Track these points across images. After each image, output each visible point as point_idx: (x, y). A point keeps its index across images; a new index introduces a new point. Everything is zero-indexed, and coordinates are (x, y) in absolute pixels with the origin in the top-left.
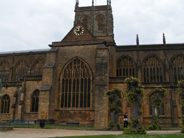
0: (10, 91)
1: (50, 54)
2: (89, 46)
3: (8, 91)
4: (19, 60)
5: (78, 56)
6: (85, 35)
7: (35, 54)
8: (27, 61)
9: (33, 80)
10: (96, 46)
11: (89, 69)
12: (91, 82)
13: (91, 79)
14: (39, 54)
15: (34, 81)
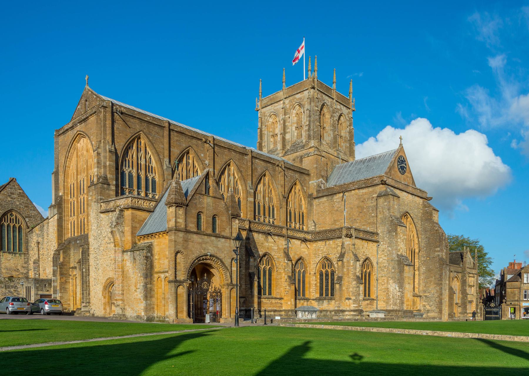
0: (273, 245)
1: (393, 200)
2: (417, 198)
3: (270, 244)
4: (225, 160)
5: (409, 212)
6: (407, 177)
7: (256, 158)
8: (242, 169)
9: (362, 239)
10: (421, 201)
11: (416, 236)
12: (416, 255)
13: (417, 251)
14: (264, 161)
15: (364, 241)
